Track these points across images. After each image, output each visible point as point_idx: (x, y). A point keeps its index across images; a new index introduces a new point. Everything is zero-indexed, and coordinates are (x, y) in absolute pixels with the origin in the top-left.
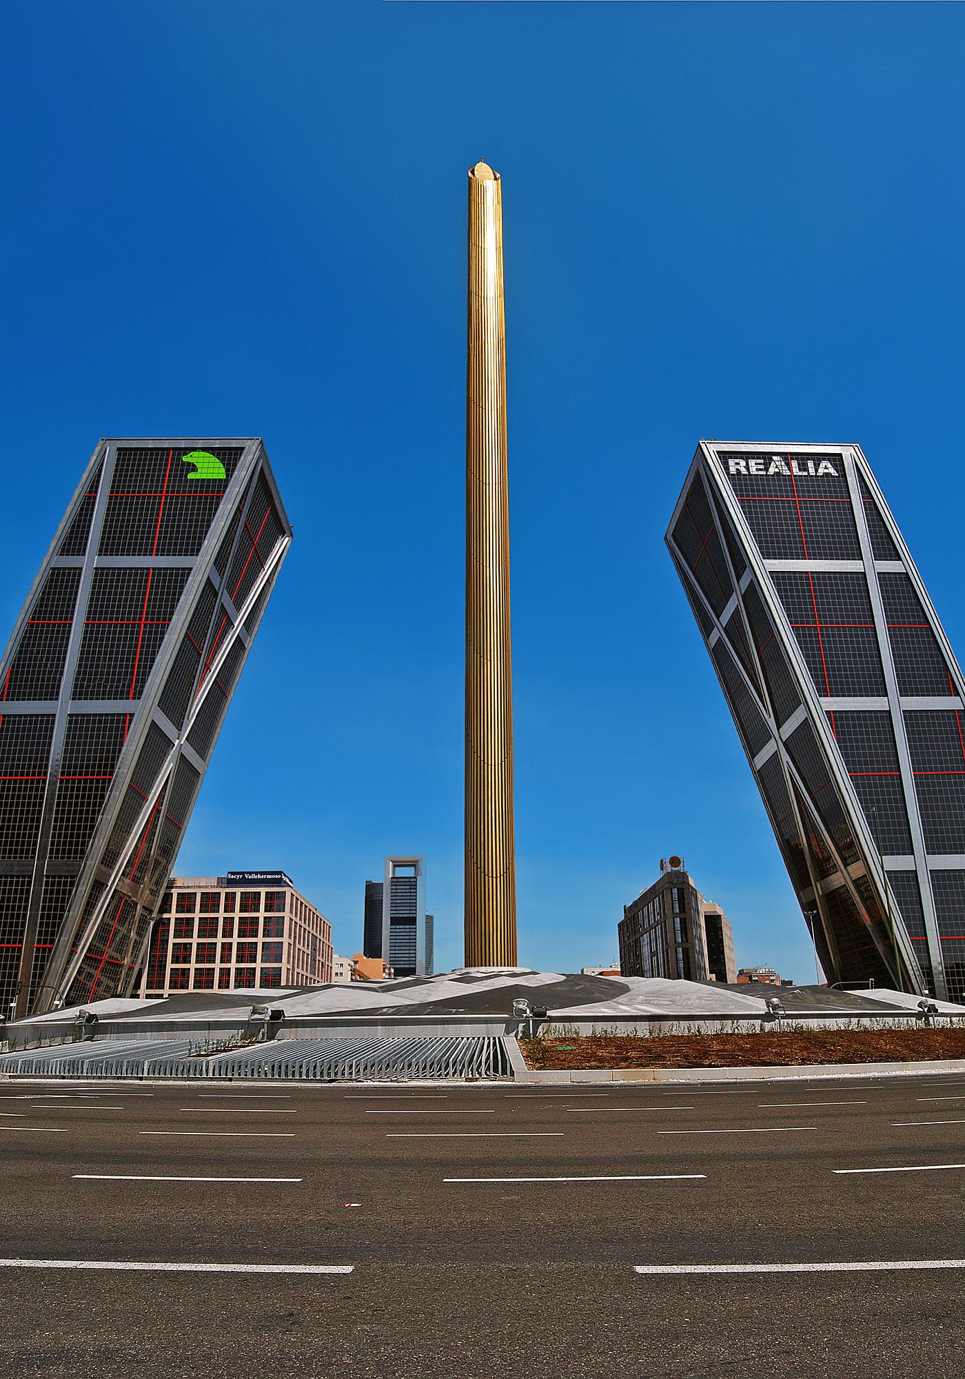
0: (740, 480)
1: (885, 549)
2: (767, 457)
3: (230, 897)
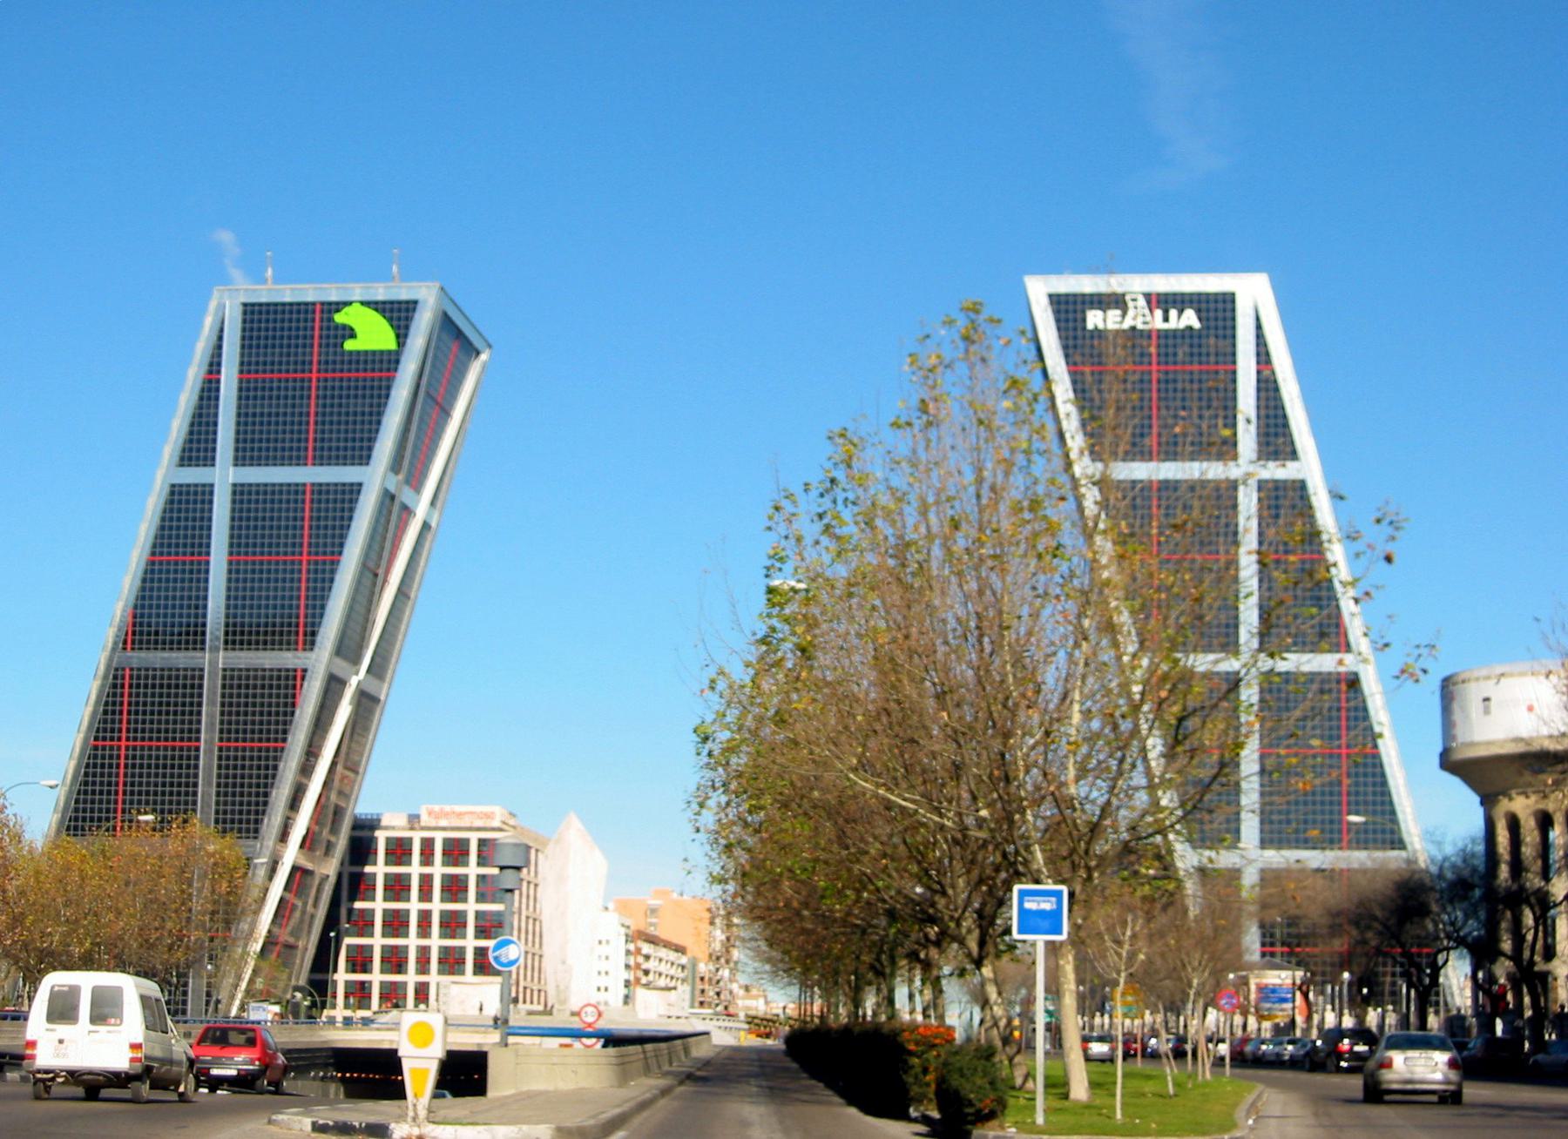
1: (1276, 438)
3: (428, 846)
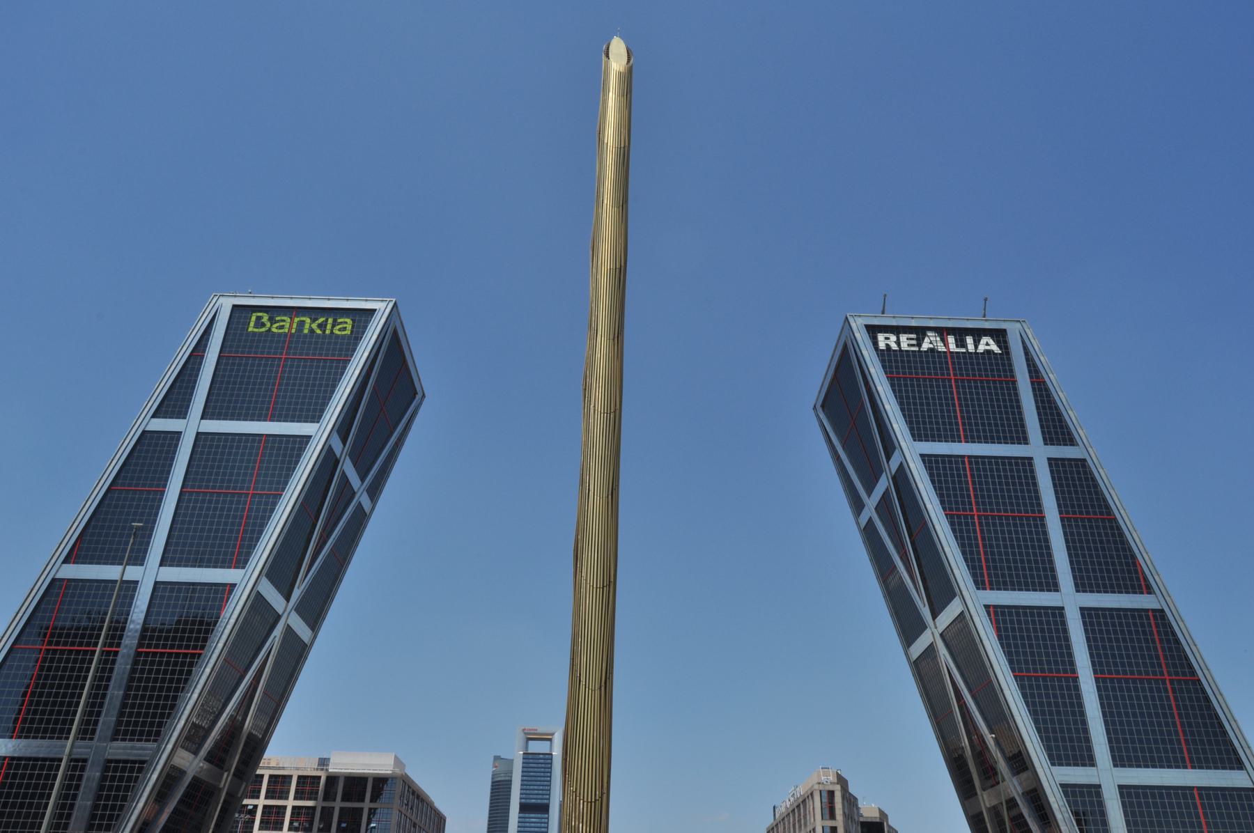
0: (889, 355)
2: (920, 332)
